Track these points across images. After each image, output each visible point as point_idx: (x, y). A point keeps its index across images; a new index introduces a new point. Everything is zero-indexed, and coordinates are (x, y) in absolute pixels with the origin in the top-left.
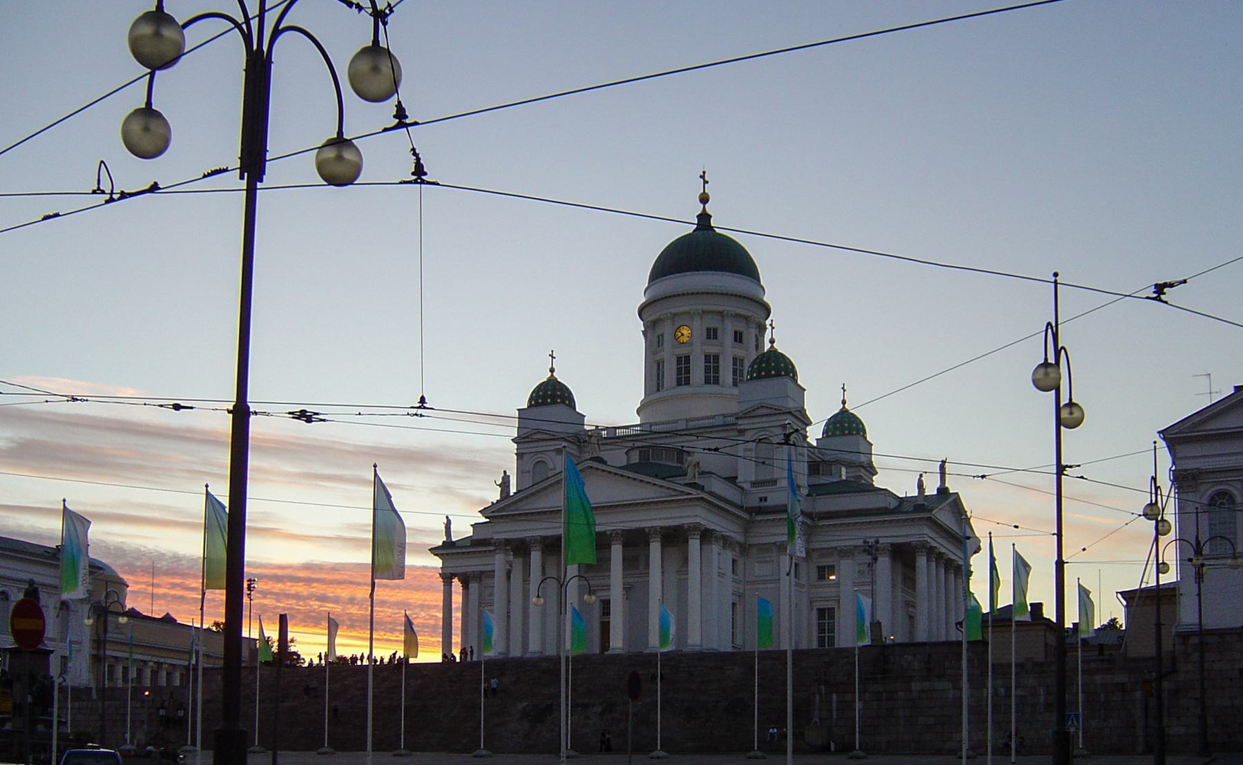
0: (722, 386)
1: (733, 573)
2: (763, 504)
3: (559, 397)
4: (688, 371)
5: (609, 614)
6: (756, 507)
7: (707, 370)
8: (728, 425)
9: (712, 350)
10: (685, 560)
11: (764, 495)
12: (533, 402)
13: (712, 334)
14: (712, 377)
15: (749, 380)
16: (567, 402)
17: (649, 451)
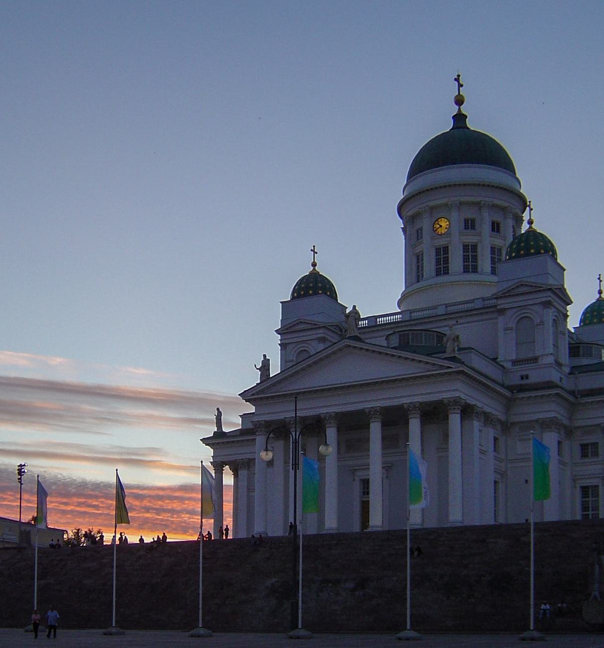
0: (480, 274)
1: (495, 451)
2: (524, 382)
3: (321, 288)
4: (446, 261)
5: (368, 493)
6: (517, 386)
7: (466, 259)
8: (488, 307)
9: (470, 239)
10: (446, 436)
11: (524, 373)
12: (295, 295)
13: (470, 224)
14: (470, 265)
15: (508, 260)
16: (328, 293)
17: (408, 334)
